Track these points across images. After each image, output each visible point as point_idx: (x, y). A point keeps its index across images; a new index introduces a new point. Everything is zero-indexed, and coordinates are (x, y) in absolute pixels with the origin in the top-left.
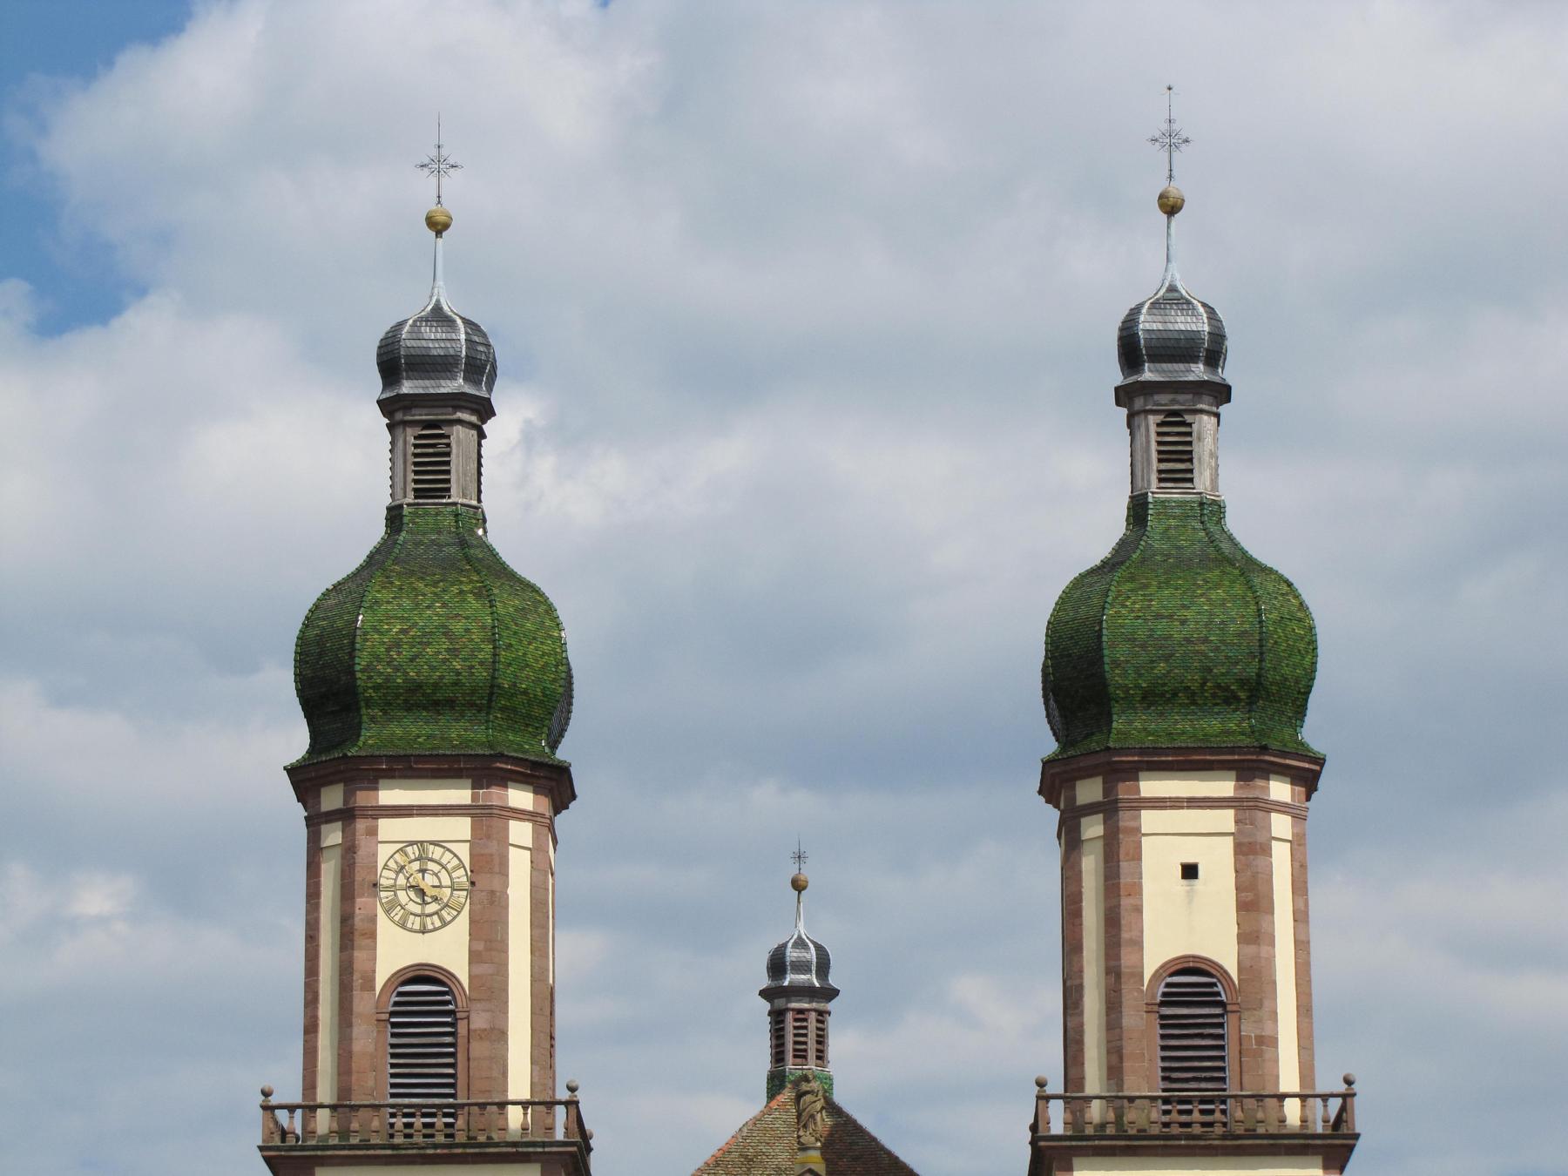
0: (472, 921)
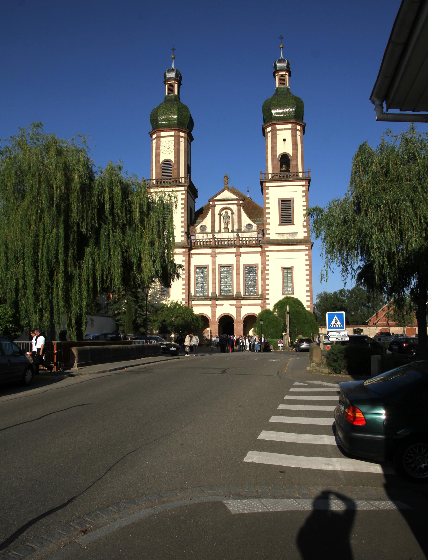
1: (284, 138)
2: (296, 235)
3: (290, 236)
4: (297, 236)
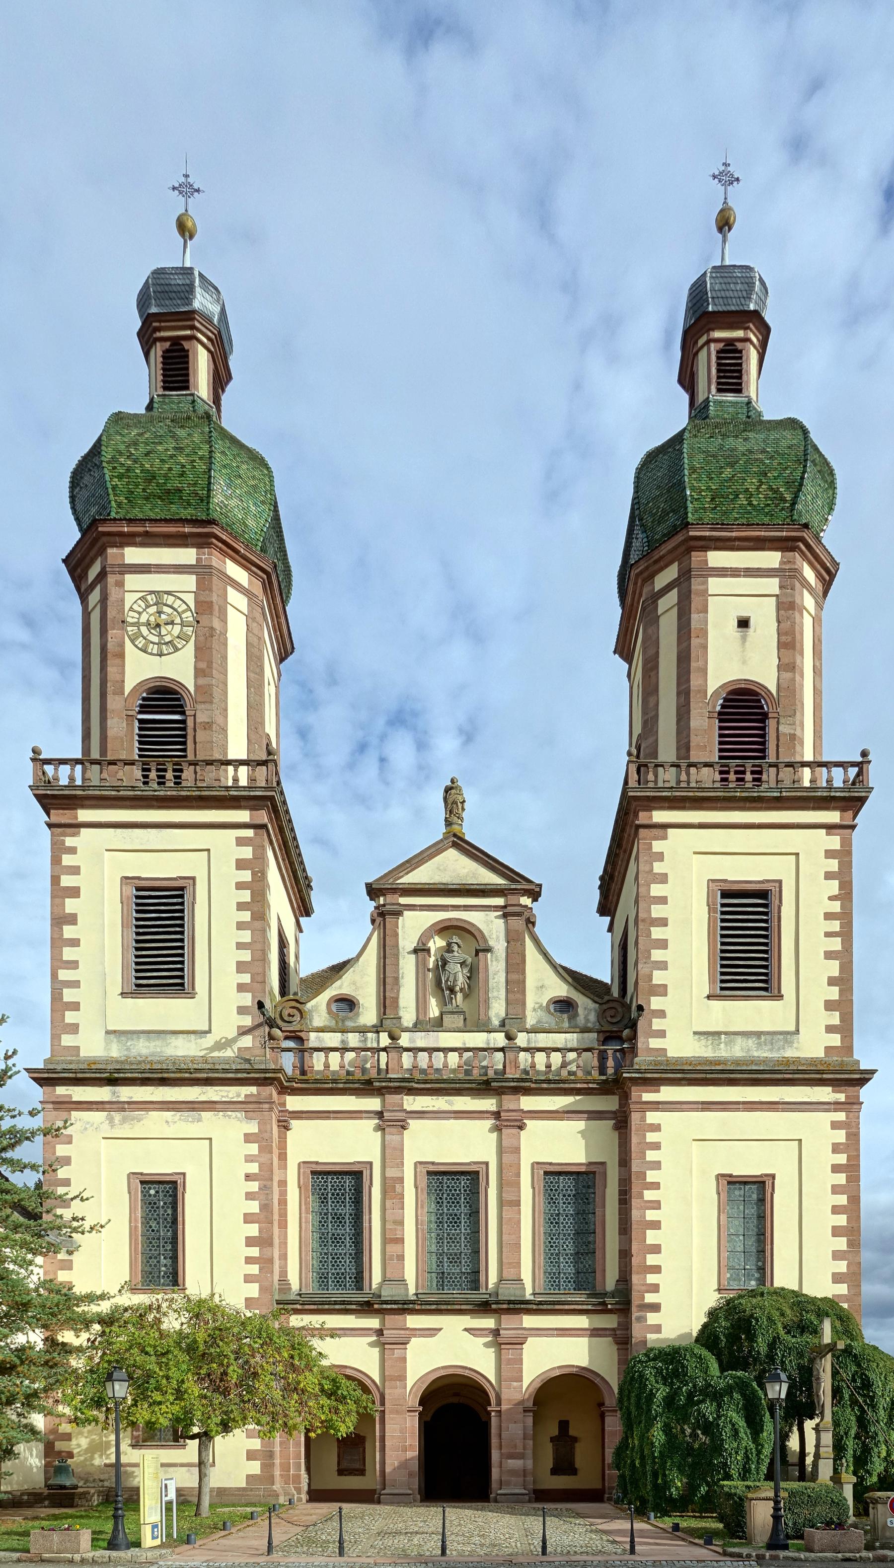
0: (197, 649)
2: (790, 1044)
3: (759, 1044)
4: (795, 1045)
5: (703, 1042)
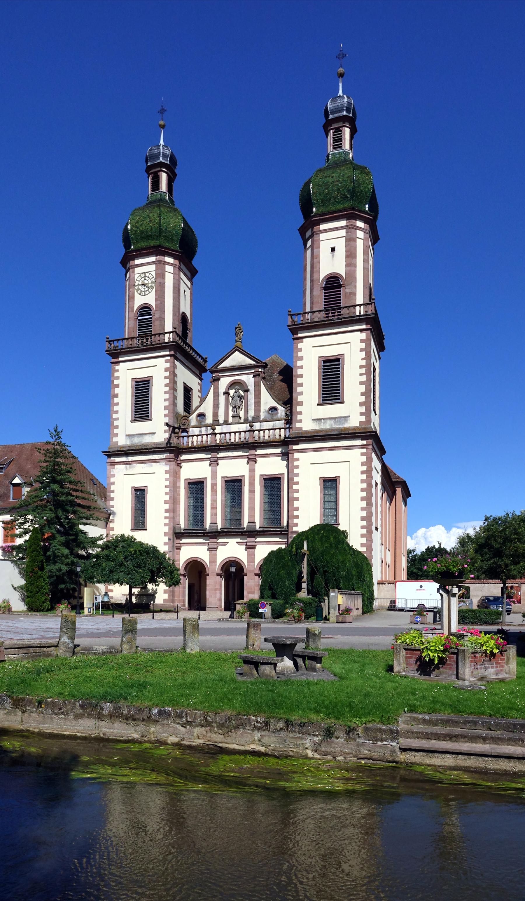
0: (156, 291)
1: (333, 246)
2: (346, 421)
5: (315, 423)
